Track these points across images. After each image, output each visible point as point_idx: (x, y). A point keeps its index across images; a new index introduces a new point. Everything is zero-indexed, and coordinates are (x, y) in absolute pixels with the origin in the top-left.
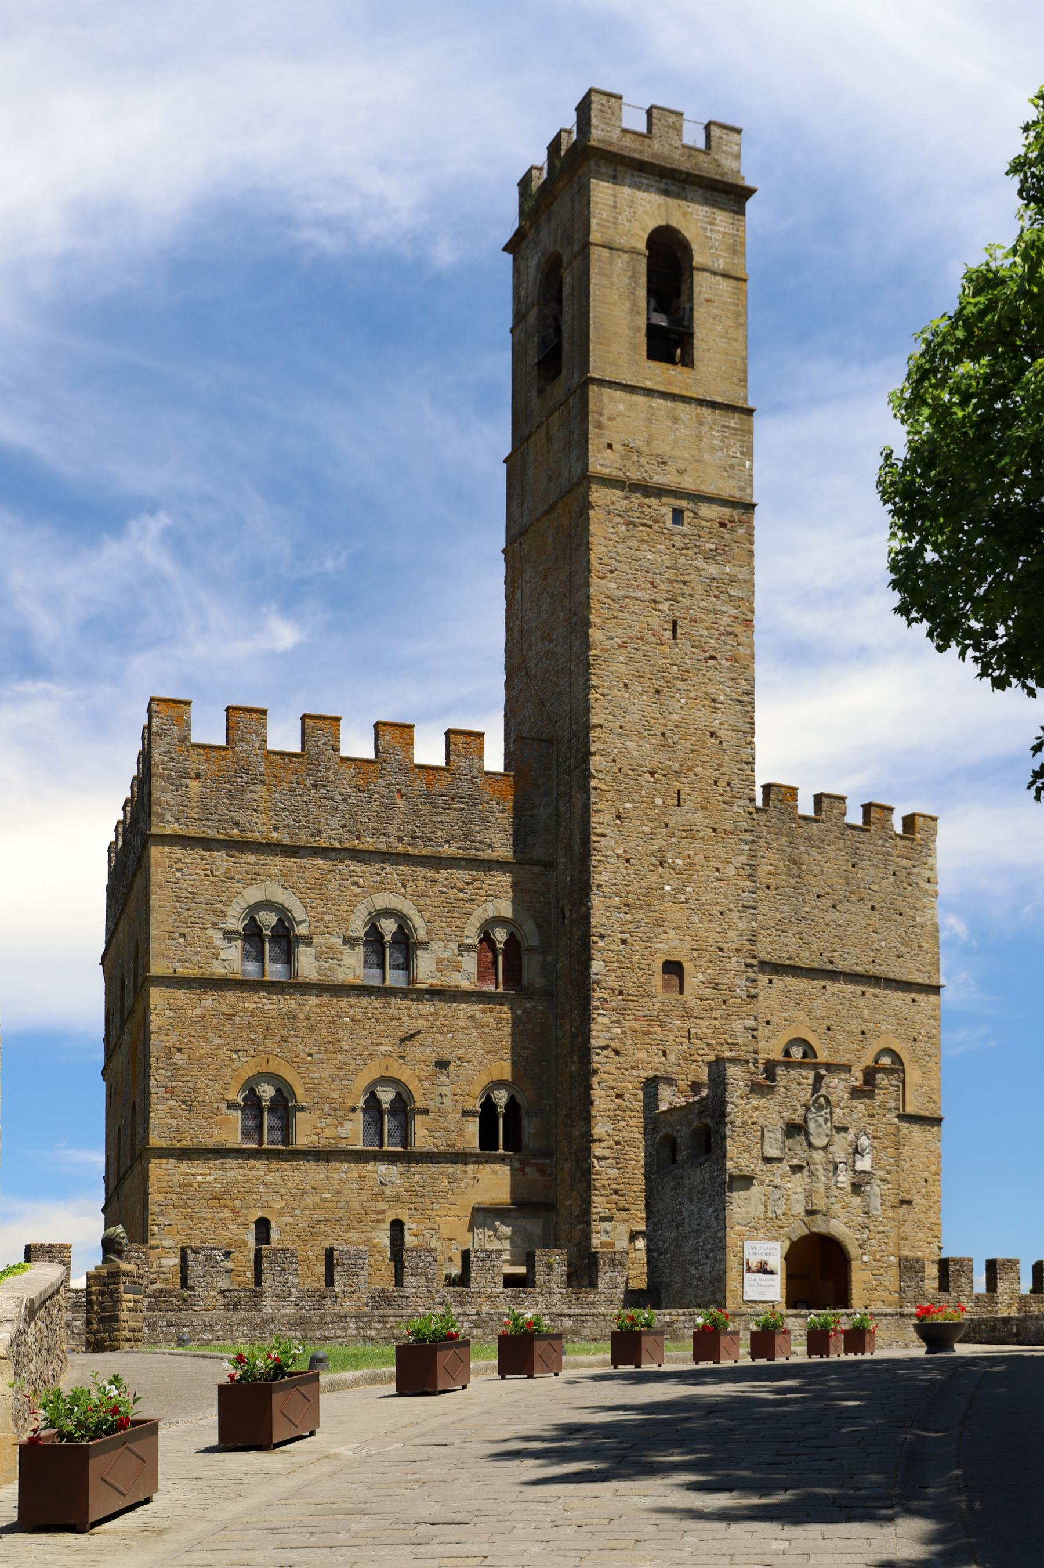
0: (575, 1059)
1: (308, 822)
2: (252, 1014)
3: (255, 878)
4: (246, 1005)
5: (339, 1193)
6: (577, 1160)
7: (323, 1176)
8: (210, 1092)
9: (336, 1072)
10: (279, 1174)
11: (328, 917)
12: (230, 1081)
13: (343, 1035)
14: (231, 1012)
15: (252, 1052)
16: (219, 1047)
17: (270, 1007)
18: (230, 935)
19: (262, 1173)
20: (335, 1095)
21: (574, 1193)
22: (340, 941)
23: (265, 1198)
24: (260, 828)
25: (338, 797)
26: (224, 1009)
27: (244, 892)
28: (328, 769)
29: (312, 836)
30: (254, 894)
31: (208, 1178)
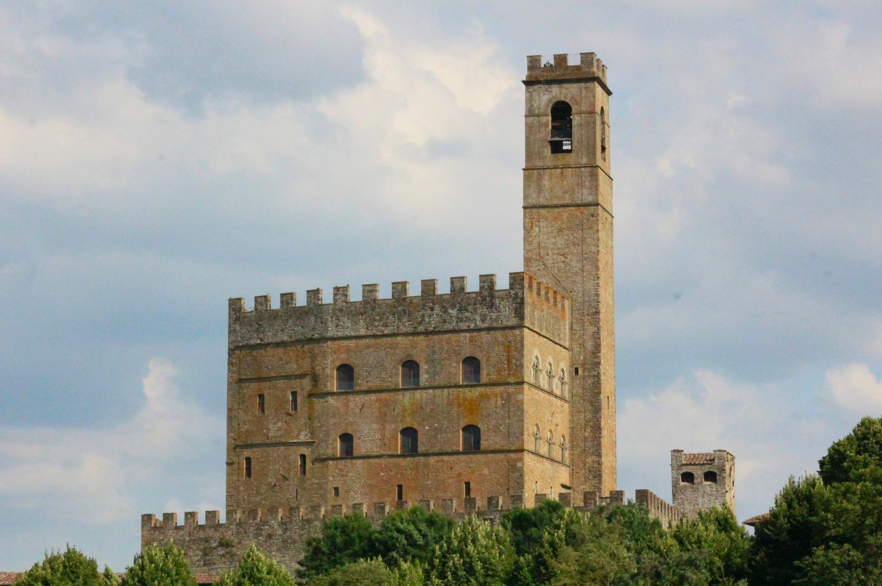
0: (589, 431)
6: (590, 471)
21: (588, 484)
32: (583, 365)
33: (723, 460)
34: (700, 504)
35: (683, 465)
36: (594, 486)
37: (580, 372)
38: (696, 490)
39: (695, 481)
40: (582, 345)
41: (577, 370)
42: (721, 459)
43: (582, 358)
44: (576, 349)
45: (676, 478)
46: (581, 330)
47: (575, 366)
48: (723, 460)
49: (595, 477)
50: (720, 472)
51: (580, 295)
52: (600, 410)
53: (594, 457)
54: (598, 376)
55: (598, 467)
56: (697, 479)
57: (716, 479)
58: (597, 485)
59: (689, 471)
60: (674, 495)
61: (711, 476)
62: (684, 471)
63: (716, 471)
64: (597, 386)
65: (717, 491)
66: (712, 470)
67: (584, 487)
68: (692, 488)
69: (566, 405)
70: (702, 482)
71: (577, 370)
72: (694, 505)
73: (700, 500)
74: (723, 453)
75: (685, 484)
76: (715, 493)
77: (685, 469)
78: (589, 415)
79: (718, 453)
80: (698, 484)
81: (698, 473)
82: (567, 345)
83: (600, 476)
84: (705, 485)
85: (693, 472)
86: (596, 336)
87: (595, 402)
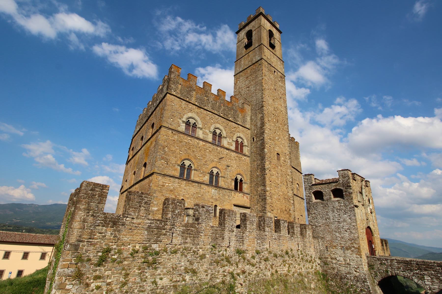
0: (259, 171)
1: (204, 103)
2: (186, 143)
3: (191, 111)
4: (185, 140)
5: (203, 195)
7: (199, 190)
8: (173, 160)
9: (205, 163)
10: (188, 187)
11: (206, 125)
12: (179, 159)
13: (207, 154)
14: (181, 141)
15: (185, 152)
16: (177, 149)
17: (191, 142)
18: (183, 122)
19: (184, 186)
20: (204, 169)
22: (208, 131)
23: (184, 193)
24: (193, 100)
25: (210, 100)
26: (180, 140)
27: (188, 113)
28: (209, 94)
29: (204, 106)
30: (190, 115)
31: (169, 185)
32: (256, 136)
33: (347, 178)
34: (331, 218)
35: (313, 185)
36: (262, 206)
37: (255, 139)
38: (325, 206)
39: (325, 198)
40: (256, 125)
41: (253, 138)
42: (344, 177)
43: (256, 132)
44: (253, 128)
45: (309, 196)
46: (255, 118)
47: (253, 137)
48: (347, 178)
49: (263, 200)
50: (346, 189)
51: (255, 101)
52: (264, 158)
53: (262, 187)
54: (263, 139)
55: (264, 193)
56: (326, 196)
57: (343, 195)
58: (263, 205)
59: (319, 190)
60: (308, 211)
61: (338, 193)
62: (314, 190)
63: (341, 188)
64: (263, 145)
65: (346, 206)
66: (338, 187)
67: (257, 207)
68: (322, 204)
69: (248, 158)
70: (330, 198)
71: (253, 138)
72: (326, 219)
73: (330, 214)
74: (346, 172)
75: (318, 201)
76: (344, 208)
77: (315, 189)
78: (259, 162)
79: (342, 172)
80: (327, 200)
81: (327, 191)
82: (248, 126)
83: (265, 199)
84: (333, 201)
85: (322, 191)
86: (262, 119)
87: (262, 154)
